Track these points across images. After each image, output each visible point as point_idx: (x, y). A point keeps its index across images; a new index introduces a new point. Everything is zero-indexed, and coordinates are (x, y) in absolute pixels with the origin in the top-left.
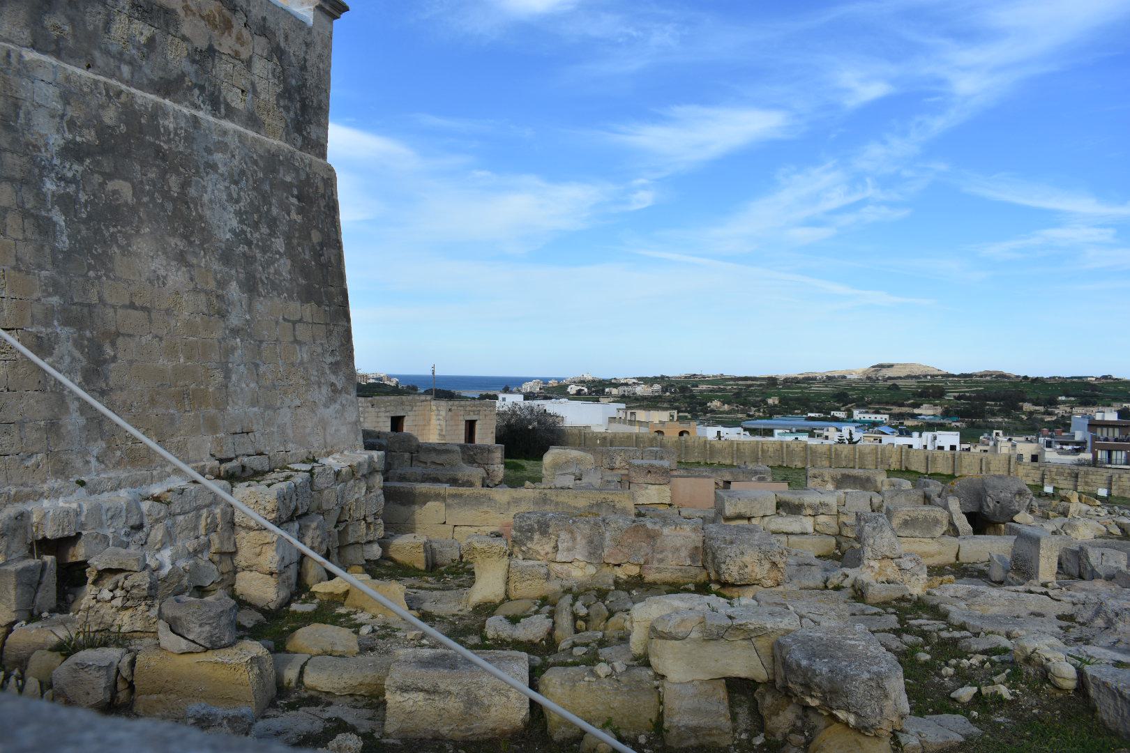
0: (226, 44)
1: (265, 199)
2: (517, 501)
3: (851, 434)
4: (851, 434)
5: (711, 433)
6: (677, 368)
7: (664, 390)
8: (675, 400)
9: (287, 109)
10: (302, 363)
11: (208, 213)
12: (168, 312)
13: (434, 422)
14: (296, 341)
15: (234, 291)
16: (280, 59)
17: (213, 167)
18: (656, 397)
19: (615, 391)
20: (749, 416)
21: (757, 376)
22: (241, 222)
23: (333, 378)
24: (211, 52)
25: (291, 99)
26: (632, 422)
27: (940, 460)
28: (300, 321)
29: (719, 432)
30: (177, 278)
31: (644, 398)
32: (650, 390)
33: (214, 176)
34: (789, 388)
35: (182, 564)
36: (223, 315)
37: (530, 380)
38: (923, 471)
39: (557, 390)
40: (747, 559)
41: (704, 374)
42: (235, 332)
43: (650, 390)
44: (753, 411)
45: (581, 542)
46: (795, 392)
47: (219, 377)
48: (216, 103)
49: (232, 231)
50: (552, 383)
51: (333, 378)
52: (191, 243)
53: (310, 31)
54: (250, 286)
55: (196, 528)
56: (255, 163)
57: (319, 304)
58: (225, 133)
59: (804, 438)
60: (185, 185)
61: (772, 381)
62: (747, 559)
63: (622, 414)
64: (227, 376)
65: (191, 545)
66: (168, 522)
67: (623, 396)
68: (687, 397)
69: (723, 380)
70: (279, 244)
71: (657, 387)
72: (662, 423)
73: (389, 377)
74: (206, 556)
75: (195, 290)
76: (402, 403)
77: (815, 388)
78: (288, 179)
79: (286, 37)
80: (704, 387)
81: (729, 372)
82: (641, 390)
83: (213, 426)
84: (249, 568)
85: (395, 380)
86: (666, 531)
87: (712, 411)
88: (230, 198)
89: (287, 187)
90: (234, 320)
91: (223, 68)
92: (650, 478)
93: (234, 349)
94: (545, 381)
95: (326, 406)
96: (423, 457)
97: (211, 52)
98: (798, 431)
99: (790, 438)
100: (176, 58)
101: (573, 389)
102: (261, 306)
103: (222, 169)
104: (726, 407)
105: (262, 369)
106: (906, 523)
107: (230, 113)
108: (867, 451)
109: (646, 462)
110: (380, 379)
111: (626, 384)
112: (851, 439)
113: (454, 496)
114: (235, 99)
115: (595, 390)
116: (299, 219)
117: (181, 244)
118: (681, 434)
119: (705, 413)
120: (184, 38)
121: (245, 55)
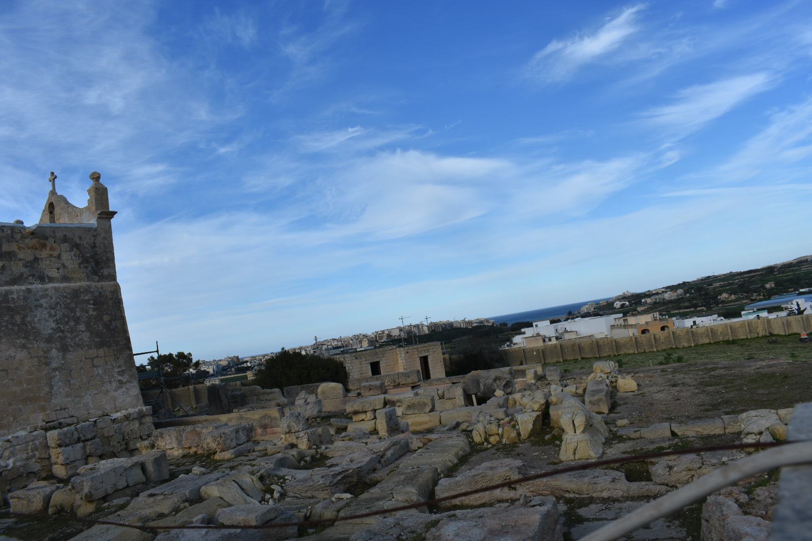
0: (44, 254)
1: (72, 310)
2: (230, 420)
3: (798, 305)
4: (798, 305)
5: (688, 323)
6: (692, 276)
7: (686, 292)
8: (694, 299)
9: (86, 268)
10: (98, 374)
11: (37, 325)
12: (17, 369)
13: (400, 361)
14: (94, 366)
15: (54, 353)
16: (78, 248)
17: (41, 306)
18: (679, 299)
19: (649, 300)
20: (752, 300)
21: (742, 270)
22: (58, 323)
23: (120, 378)
24: (36, 259)
25: (87, 262)
26: (625, 327)
27: (794, 323)
28: (97, 357)
29: (694, 322)
30: (22, 355)
31: (670, 302)
32: (675, 294)
33: (40, 310)
34: (783, 272)
35: (18, 464)
36: (47, 364)
37: (585, 304)
38: (783, 333)
39: (571, 313)
40: (208, 440)
41: (716, 274)
42: (55, 370)
43: (675, 294)
44: (755, 296)
45: (174, 439)
46: (790, 274)
47: (47, 389)
48: (42, 279)
49: (53, 329)
50: (603, 303)
51: (120, 378)
52: (28, 340)
53: (95, 230)
54: (64, 349)
55: (27, 450)
56: (66, 297)
57: (109, 347)
58: (46, 290)
59: (764, 314)
60: (23, 319)
61: (770, 270)
62: (208, 440)
63: (618, 322)
64: (51, 387)
65: (24, 456)
66: (12, 449)
67: (655, 303)
68: (700, 295)
69: (731, 276)
70: (82, 327)
71: (680, 291)
72: (647, 323)
73: (487, 320)
74: (33, 460)
75: (31, 357)
76: (376, 354)
77: (804, 269)
78: (87, 298)
79: (80, 238)
80: (717, 284)
81: (736, 270)
82: (667, 296)
83: (43, 409)
84: (55, 463)
85: (492, 321)
86: (204, 431)
87: (723, 302)
88: (50, 316)
89: (87, 302)
90: (54, 365)
91: (43, 265)
92: (371, 392)
93: (54, 377)
94: (597, 303)
95: (115, 391)
96: (261, 398)
97: (36, 259)
98: (759, 310)
99: (752, 317)
100: (17, 268)
101: (617, 305)
102: (70, 356)
103: (45, 305)
104: (733, 297)
105: (72, 382)
106: (409, 407)
107: (51, 280)
108: (737, 326)
109: (367, 384)
110: (481, 322)
111: (657, 294)
112: (799, 308)
113: (206, 421)
114: (54, 273)
115: (602, 309)
116: (95, 313)
117: (23, 341)
118: (663, 328)
119: (717, 305)
120: (20, 260)
121: (55, 253)
